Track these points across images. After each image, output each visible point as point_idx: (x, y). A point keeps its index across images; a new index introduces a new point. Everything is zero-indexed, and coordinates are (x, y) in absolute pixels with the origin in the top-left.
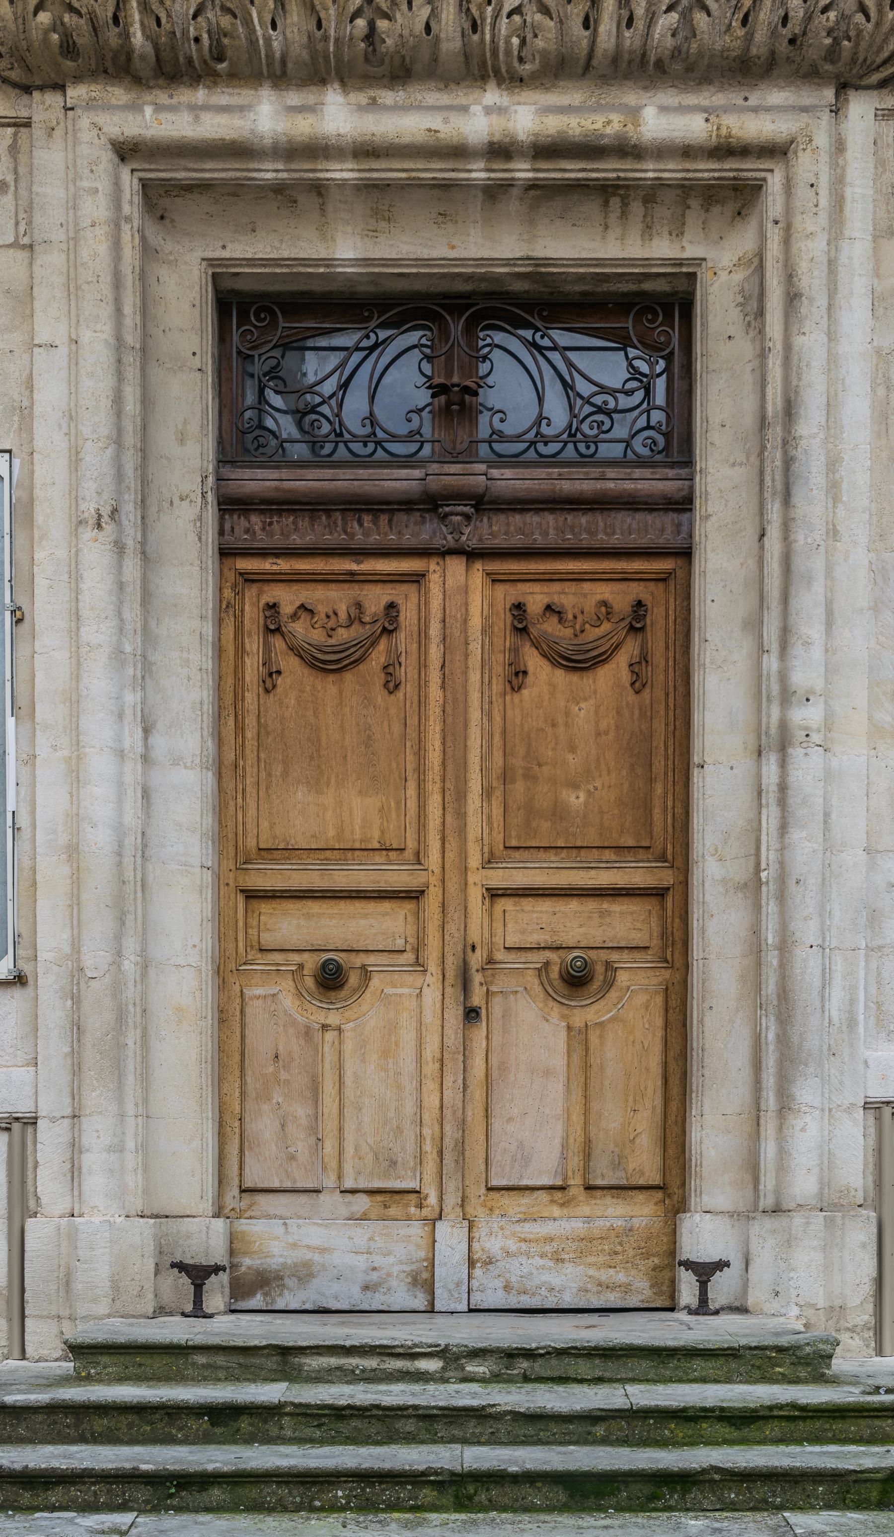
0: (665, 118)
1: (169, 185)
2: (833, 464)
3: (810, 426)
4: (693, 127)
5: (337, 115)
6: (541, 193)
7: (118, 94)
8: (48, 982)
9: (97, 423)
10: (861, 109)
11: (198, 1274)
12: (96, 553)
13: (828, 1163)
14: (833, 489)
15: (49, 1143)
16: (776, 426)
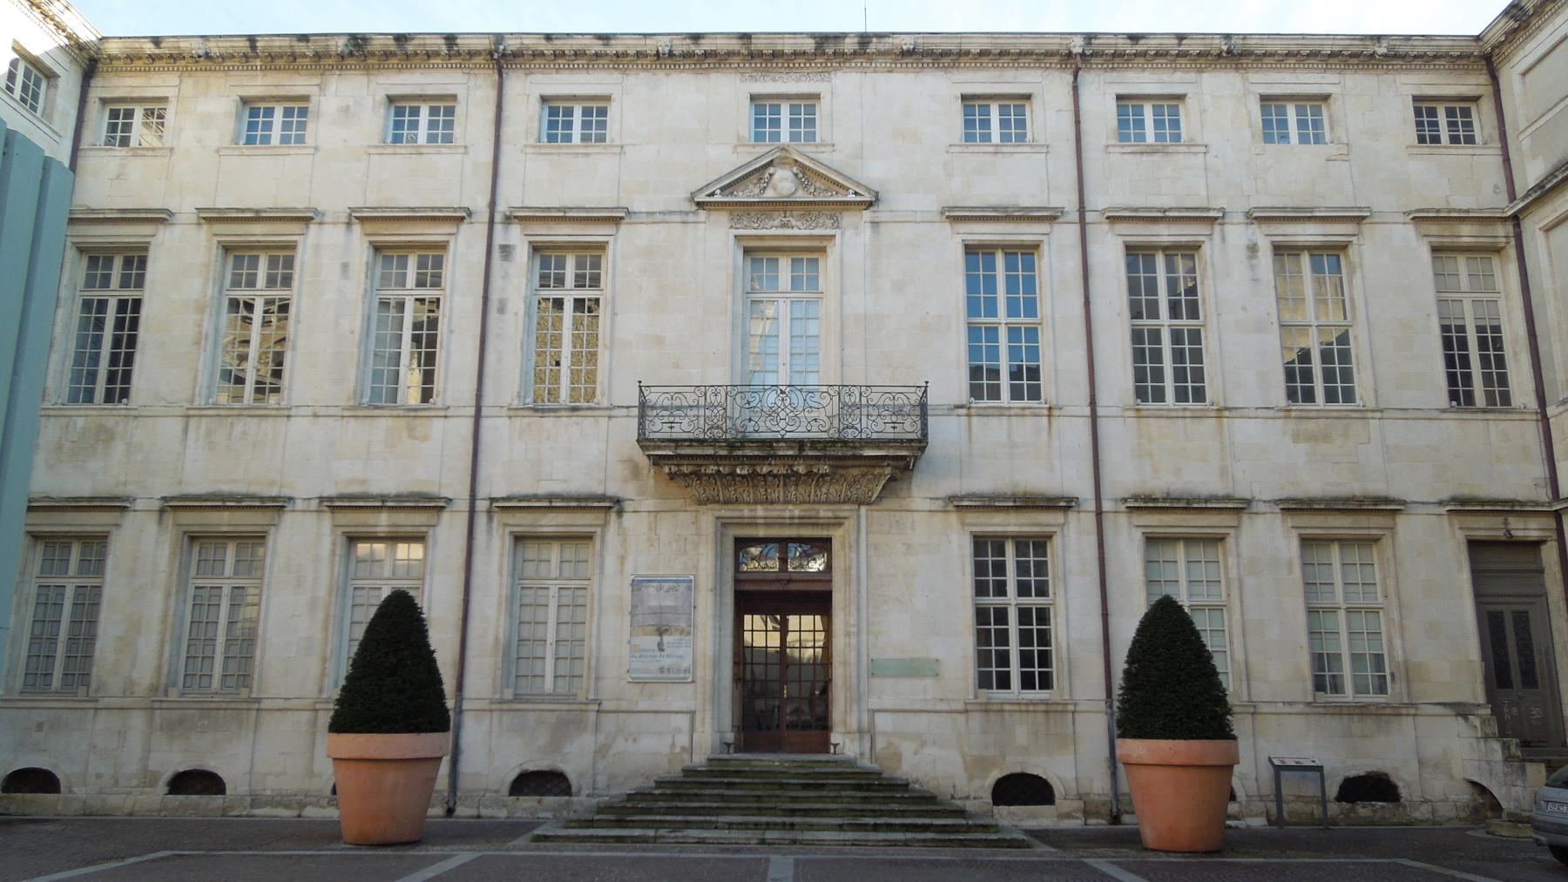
0: (824, 512)
1: (724, 524)
2: (859, 578)
3: (854, 572)
4: (830, 514)
5: (760, 511)
6: (799, 525)
7: (717, 506)
8: (699, 683)
9: (711, 570)
10: (863, 509)
11: (728, 745)
12: (710, 596)
13: (860, 721)
14: (859, 584)
15: (698, 717)
16: (847, 570)
